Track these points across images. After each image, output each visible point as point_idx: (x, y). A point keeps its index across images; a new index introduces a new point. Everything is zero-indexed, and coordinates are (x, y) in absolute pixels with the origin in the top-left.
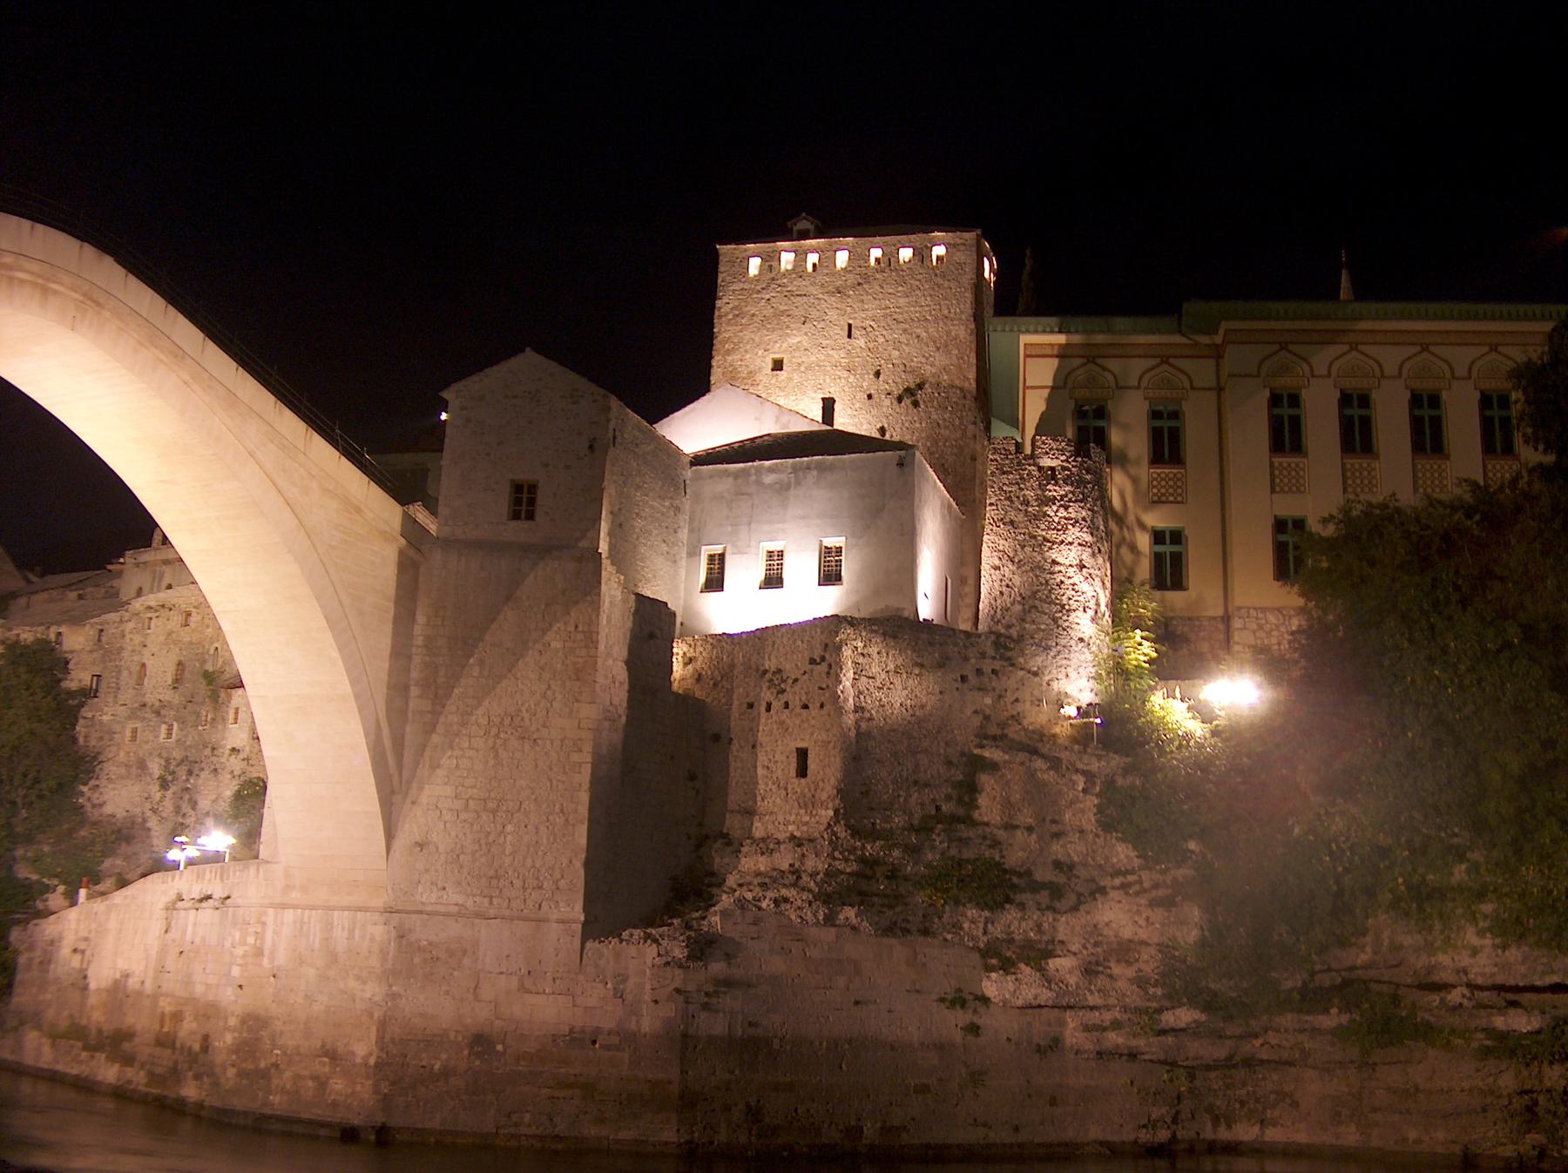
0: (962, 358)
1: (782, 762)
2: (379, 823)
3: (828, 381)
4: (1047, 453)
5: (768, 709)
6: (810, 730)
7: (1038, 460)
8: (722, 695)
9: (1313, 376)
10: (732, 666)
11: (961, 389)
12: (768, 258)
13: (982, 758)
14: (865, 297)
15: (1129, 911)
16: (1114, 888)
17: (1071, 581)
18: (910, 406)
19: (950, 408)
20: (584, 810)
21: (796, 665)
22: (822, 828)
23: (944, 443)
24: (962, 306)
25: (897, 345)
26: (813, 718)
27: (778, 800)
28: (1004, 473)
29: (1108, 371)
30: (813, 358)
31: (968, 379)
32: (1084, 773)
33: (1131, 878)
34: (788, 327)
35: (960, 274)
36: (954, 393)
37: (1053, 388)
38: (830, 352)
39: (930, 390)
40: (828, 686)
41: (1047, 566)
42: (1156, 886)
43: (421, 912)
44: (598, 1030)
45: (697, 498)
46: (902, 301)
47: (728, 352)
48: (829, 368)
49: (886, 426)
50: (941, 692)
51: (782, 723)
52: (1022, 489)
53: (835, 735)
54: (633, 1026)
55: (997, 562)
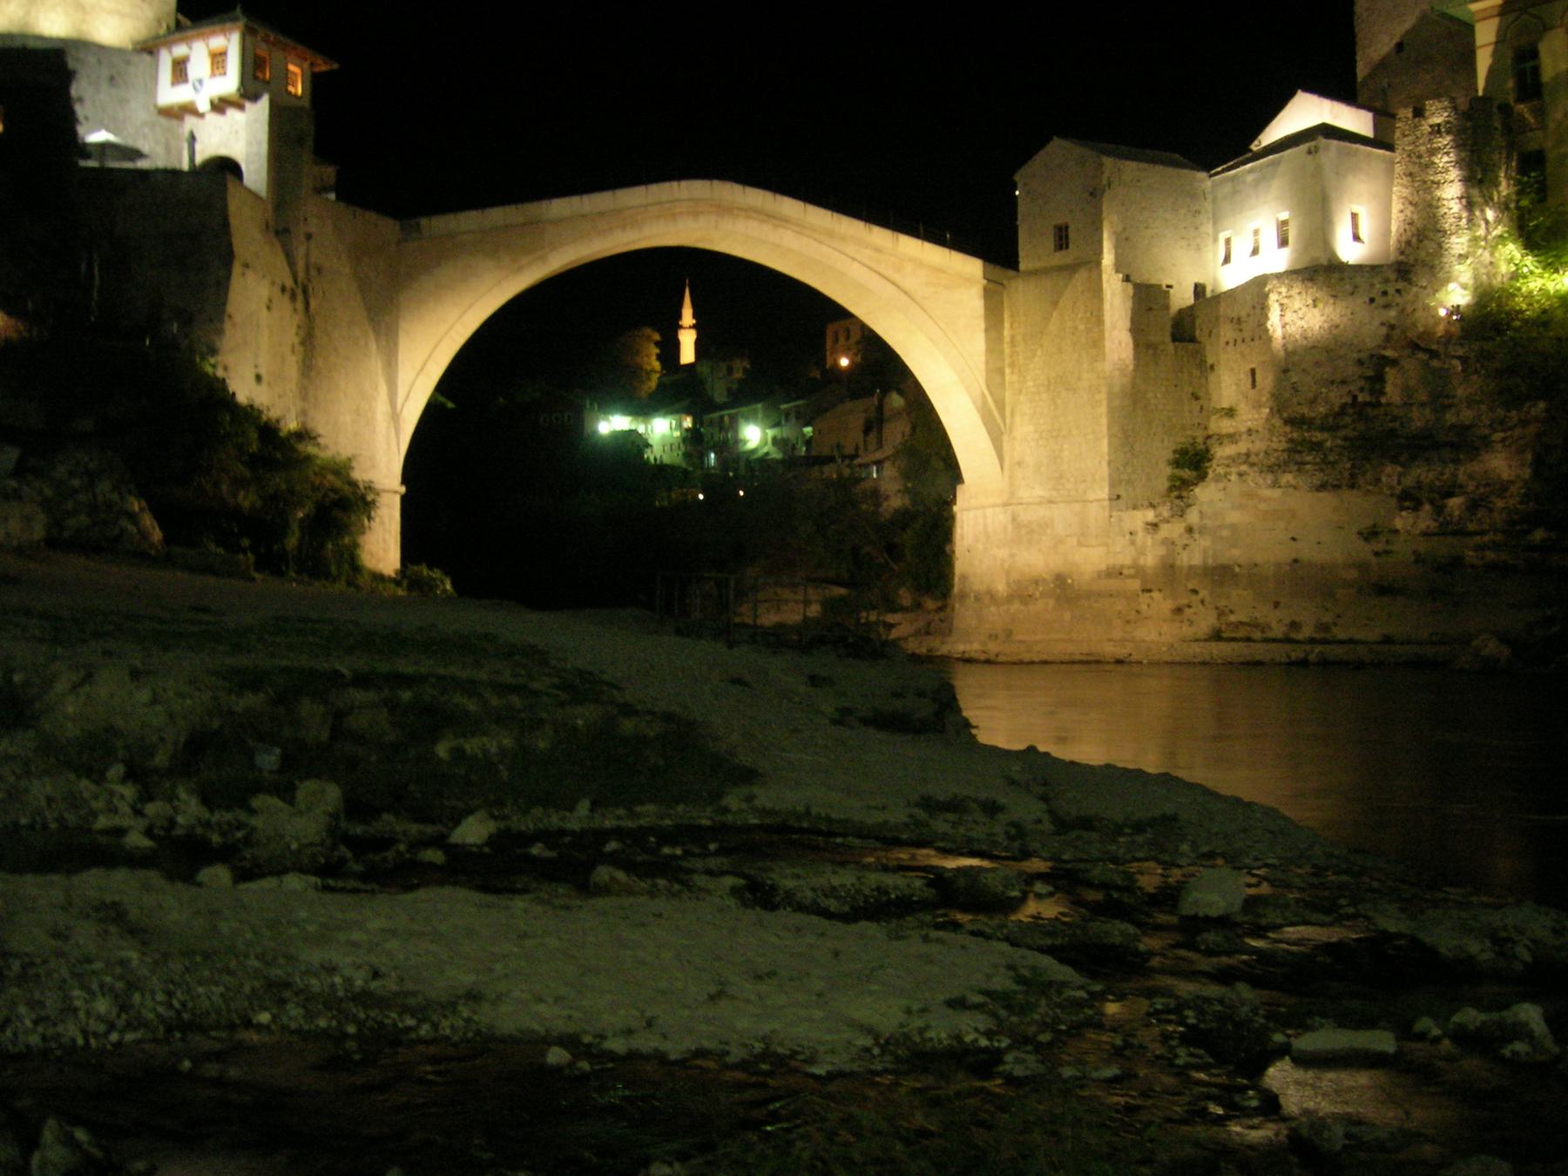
2: (993, 453)
20: (1104, 429)
22: (1263, 421)
28: (1405, 136)
32: (1459, 358)
37: (1497, 43)
41: (1434, 203)
43: (1021, 504)
44: (1122, 567)
45: (1214, 200)
50: (1352, 314)
54: (1142, 562)
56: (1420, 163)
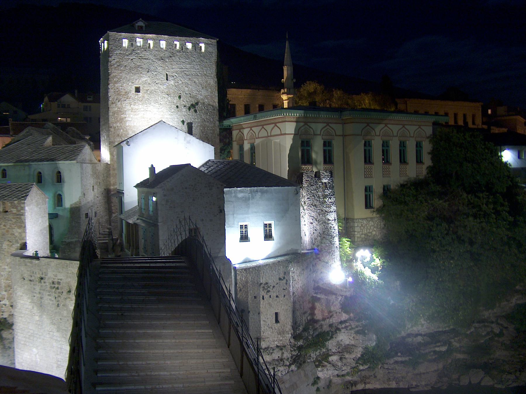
0: (212, 93)
1: (270, 318)
3: (160, 99)
4: (324, 177)
5: (263, 299)
6: (280, 306)
7: (322, 180)
8: (243, 294)
9: (376, 135)
10: (247, 282)
11: (213, 106)
12: (131, 40)
13: (316, 297)
14: (173, 63)
15: (348, 335)
16: (342, 328)
17: (333, 226)
18: (193, 112)
19: (209, 114)
21: (273, 281)
23: (207, 128)
24: (212, 71)
25: (187, 85)
26: (281, 301)
27: (269, 333)
28: (312, 186)
29: (312, 128)
30: (153, 88)
31: (215, 102)
33: (347, 324)
34: (141, 73)
35: (211, 57)
36: (210, 107)
37: (295, 134)
38: (160, 86)
39: (201, 106)
40: (286, 288)
42: (357, 327)
46: (188, 66)
47: (116, 82)
48: (160, 93)
49: (184, 120)
51: (269, 304)
52: (317, 192)
53: (289, 306)
55: (312, 221)
56: (320, 201)
